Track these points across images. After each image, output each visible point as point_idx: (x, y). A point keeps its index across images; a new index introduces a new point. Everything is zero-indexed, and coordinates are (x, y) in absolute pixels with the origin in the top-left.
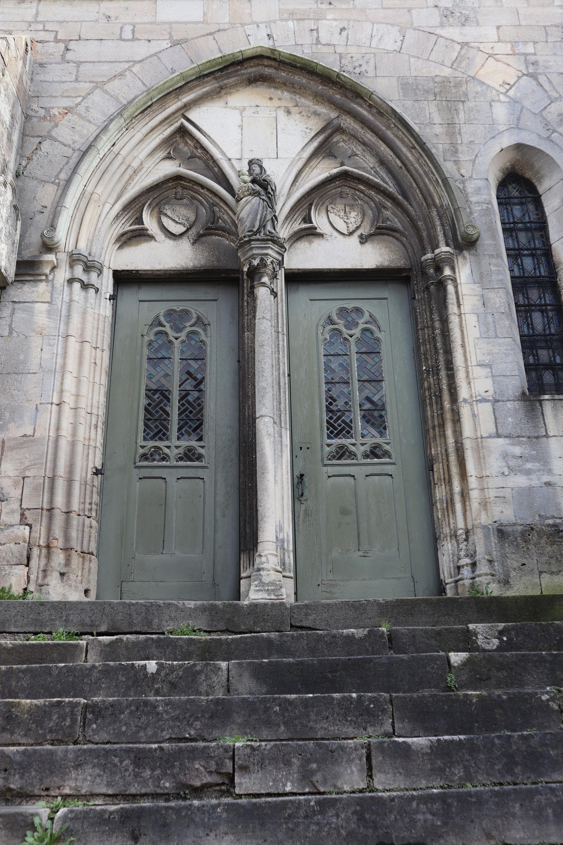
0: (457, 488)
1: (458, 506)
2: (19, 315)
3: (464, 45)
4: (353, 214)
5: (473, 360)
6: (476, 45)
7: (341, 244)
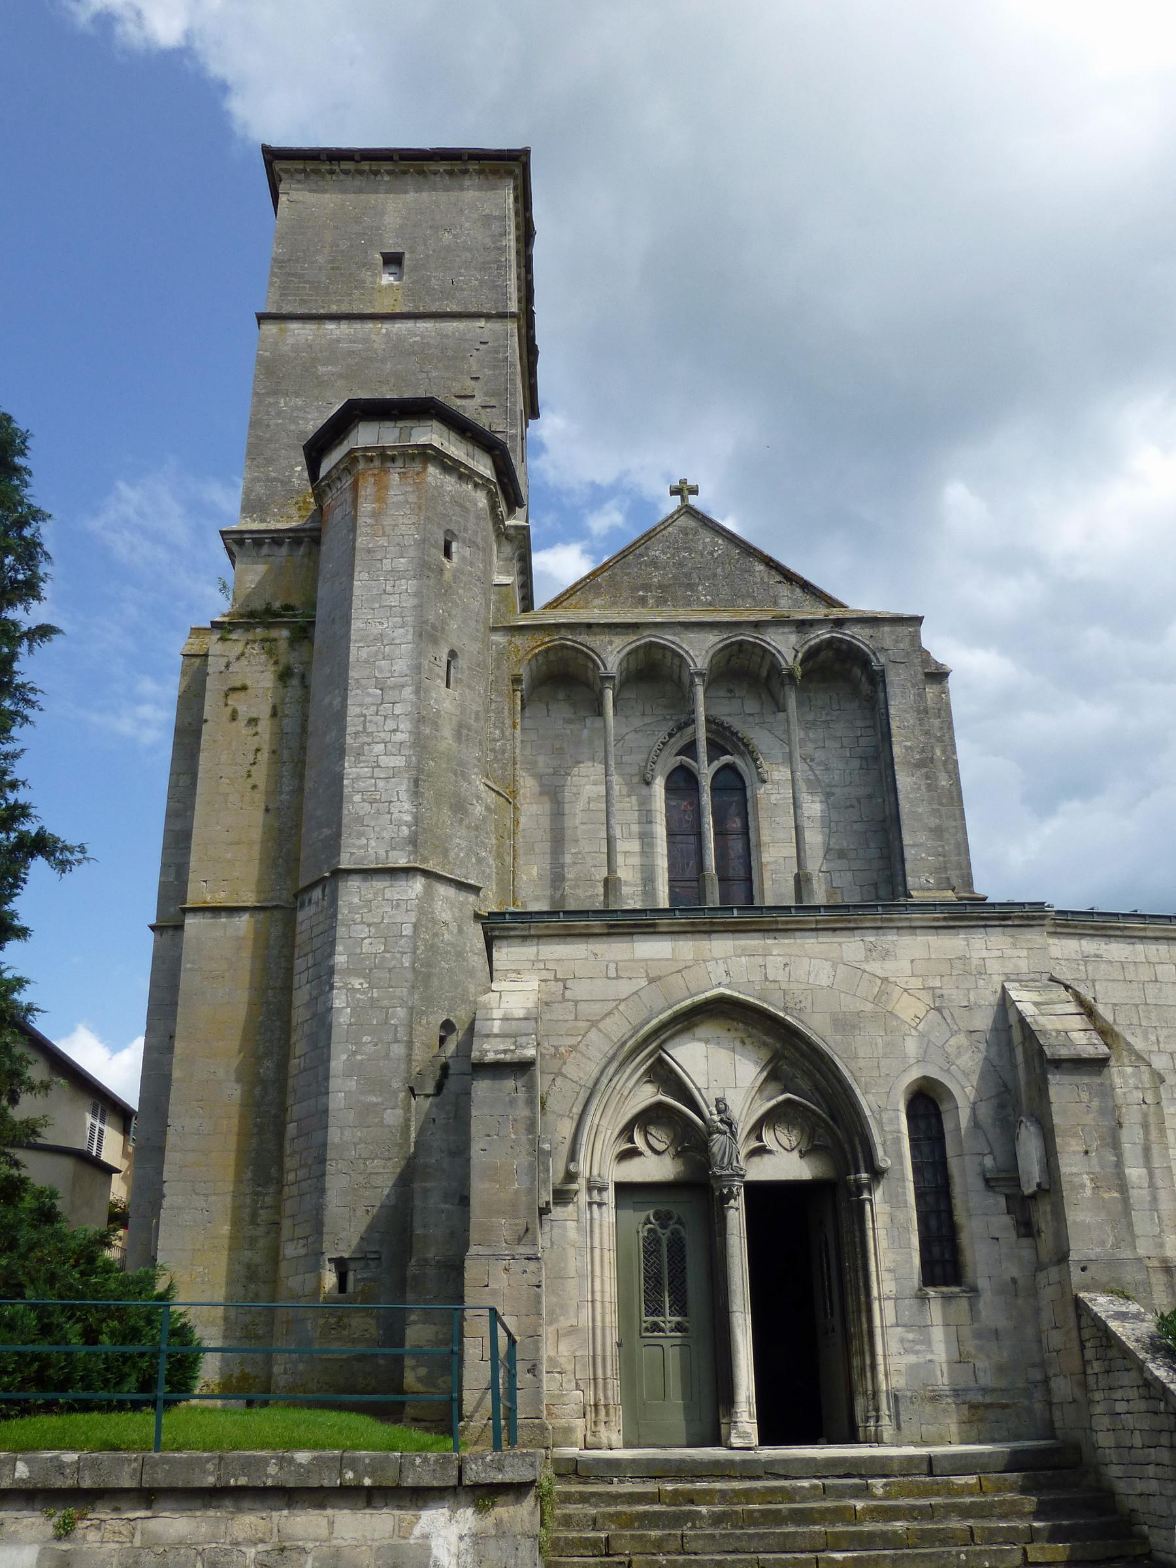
0: (868, 1362)
1: (869, 1375)
2: (556, 1231)
3: (885, 980)
4: (795, 1132)
5: (882, 1266)
6: (894, 979)
7: (785, 1163)
